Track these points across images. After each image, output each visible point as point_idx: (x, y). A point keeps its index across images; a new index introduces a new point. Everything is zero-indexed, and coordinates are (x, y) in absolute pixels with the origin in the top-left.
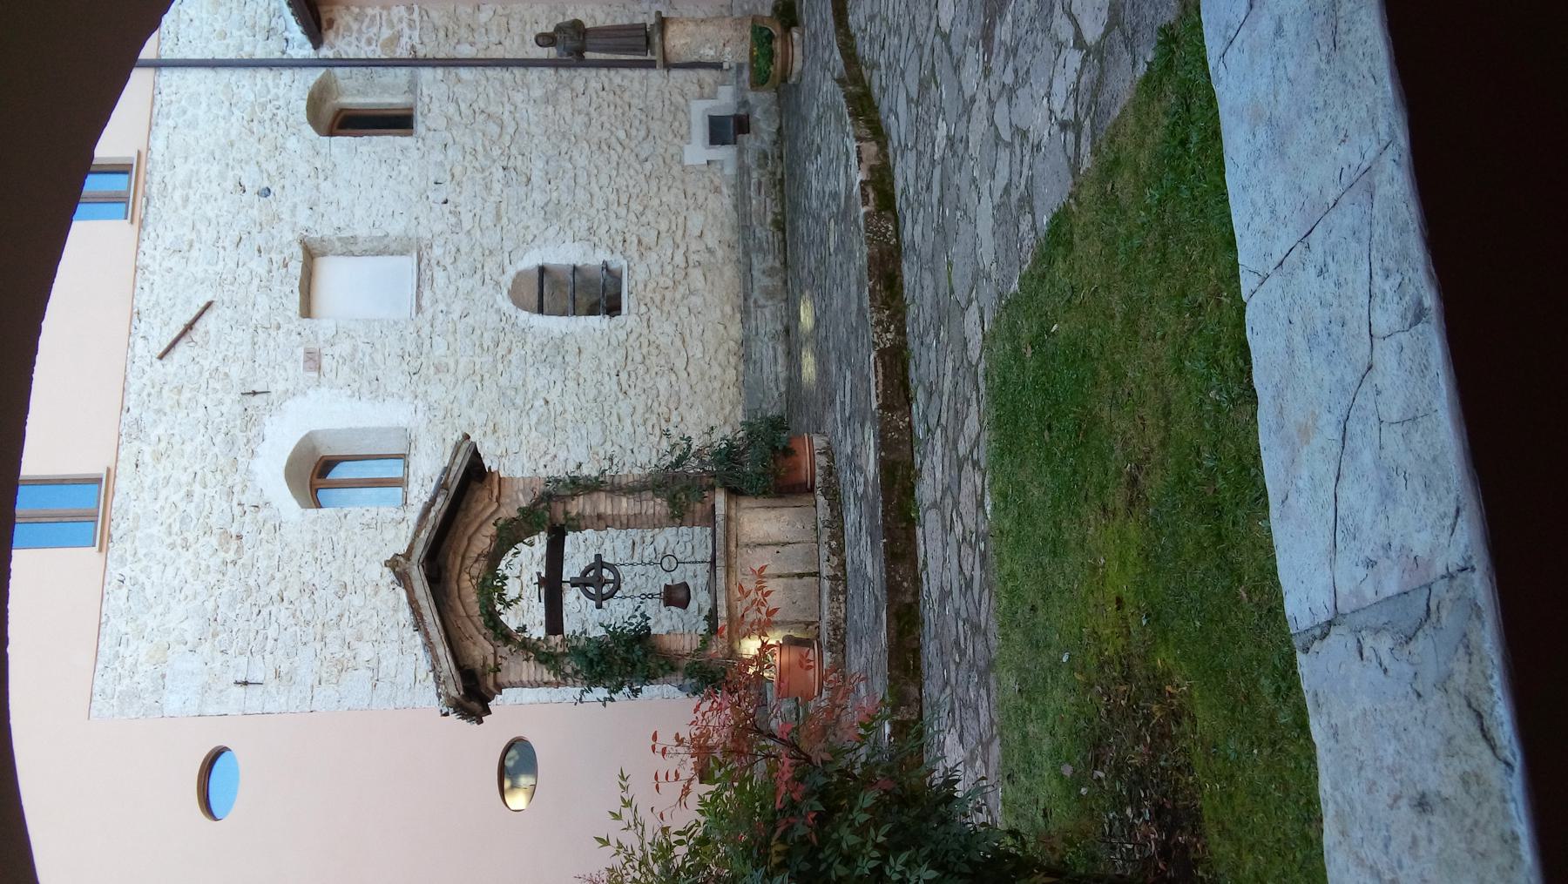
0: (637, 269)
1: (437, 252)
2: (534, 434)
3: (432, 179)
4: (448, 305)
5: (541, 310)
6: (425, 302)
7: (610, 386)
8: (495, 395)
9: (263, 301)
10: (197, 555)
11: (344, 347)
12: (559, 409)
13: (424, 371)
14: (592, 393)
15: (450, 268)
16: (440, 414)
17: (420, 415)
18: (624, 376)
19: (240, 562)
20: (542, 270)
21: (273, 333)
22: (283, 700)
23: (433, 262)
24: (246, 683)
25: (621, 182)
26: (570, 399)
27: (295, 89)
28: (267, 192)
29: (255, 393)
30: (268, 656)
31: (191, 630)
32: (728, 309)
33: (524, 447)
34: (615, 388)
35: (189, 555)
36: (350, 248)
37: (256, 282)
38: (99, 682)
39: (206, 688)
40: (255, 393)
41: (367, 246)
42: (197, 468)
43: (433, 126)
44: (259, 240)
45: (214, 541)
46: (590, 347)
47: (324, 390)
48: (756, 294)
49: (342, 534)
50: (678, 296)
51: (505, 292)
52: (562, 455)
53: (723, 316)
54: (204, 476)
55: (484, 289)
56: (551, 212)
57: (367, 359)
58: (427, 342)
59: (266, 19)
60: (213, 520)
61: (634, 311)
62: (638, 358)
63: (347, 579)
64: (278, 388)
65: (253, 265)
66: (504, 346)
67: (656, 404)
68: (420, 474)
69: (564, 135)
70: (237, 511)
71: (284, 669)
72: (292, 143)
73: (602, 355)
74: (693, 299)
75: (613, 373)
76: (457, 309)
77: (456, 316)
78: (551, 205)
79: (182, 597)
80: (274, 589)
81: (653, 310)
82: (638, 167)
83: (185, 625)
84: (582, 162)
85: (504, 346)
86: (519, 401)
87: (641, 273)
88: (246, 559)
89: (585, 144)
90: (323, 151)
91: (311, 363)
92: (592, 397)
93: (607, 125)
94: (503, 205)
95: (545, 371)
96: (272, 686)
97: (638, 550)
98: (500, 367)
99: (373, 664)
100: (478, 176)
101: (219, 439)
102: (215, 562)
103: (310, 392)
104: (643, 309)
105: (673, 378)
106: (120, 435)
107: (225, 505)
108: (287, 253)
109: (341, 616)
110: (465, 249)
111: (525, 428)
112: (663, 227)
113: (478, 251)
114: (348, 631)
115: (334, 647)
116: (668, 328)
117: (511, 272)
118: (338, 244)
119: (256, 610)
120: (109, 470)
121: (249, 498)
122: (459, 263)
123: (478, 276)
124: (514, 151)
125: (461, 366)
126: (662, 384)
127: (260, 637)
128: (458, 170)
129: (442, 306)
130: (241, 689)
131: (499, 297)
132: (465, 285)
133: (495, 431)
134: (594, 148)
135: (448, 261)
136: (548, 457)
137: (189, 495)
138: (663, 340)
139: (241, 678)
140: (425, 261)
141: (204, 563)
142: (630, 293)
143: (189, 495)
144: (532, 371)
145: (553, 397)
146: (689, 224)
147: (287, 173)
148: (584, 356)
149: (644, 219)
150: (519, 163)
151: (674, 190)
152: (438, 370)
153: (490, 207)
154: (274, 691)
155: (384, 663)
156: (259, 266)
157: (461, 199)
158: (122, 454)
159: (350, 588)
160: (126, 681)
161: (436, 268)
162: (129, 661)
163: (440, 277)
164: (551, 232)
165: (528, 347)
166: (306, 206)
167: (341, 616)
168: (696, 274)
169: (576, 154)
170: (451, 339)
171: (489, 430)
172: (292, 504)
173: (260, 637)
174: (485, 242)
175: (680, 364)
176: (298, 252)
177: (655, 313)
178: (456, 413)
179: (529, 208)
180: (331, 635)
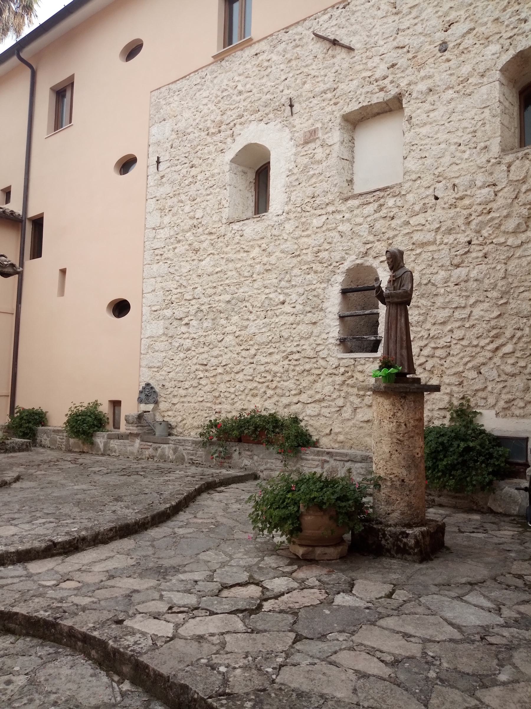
1: (391, 202)
2: (264, 297)
3: (457, 181)
4: (349, 220)
6: (350, 203)
7: (290, 347)
8: (287, 267)
12: (278, 312)
13: (304, 214)
14: (285, 334)
15: (377, 215)
16: (275, 232)
17: (275, 219)
18: (296, 356)
21: (332, 102)
22: (152, 184)
23: (382, 201)
25: (455, 349)
26: (283, 319)
30: (169, 170)
31: (181, 125)
32: (341, 438)
33: (256, 291)
34: (289, 350)
37: (369, 74)
38: (164, 88)
42: (255, 91)
43: (513, 168)
44: (402, 62)
45: (219, 118)
46: (316, 330)
47: (294, 150)
48: (332, 462)
49: (218, 190)
51: (359, 261)
52: (252, 317)
53: (337, 434)
55: (360, 244)
57: (311, 173)
58: (323, 212)
62: (307, 367)
63: (198, 200)
66: (319, 268)
67: (278, 379)
68: (245, 228)
69: (507, 293)
71: (164, 180)
72: (494, 48)
73: (311, 340)
75: (299, 349)
76: (344, 227)
77: (340, 228)
78: (434, 288)
81: (342, 378)
82: (470, 365)
84: (477, 312)
85: (319, 268)
86: (283, 283)
88: (209, 139)
90: (485, 79)
93: (519, 334)
95: (301, 300)
96: (158, 177)
97: (202, 368)
98: (305, 267)
100: (460, 221)
101: (269, 96)
102: (209, 124)
103: (292, 143)
104: (342, 370)
105: (293, 392)
106: (271, 35)
107: (234, 117)
110: (394, 223)
111: (267, 291)
113: (391, 234)
115: (170, 202)
116: (328, 389)
119: (187, 155)
120: (251, 39)
122: (382, 222)
123: (371, 238)
124: (487, 249)
125: (306, 240)
126: (290, 384)
127: (176, 162)
128: (466, 202)
129: (347, 216)
132: (363, 230)
133: (267, 271)
136: (251, 308)
138: (318, 385)
140: (381, 194)
143: (240, 93)
144: (301, 290)
145: (287, 308)
148: (310, 326)
150: (474, 255)
152: (303, 223)
153: (430, 237)
154: (156, 178)
155: (162, 231)
156: (382, 70)
157: (439, 211)
158: (263, 43)
159: (193, 203)
160: (164, 102)
161: (376, 205)
162: (171, 100)
165: (318, 285)
166: (431, 86)
169: (486, 305)
170: (324, 228)
171: (268, 267)
173: (176, 162)
174: (399, 238)
175: (303, 398)
176: (393, 91)
177: (339, 379)
178: (278, 242)
179: (431, 270)
180: (175, 200)
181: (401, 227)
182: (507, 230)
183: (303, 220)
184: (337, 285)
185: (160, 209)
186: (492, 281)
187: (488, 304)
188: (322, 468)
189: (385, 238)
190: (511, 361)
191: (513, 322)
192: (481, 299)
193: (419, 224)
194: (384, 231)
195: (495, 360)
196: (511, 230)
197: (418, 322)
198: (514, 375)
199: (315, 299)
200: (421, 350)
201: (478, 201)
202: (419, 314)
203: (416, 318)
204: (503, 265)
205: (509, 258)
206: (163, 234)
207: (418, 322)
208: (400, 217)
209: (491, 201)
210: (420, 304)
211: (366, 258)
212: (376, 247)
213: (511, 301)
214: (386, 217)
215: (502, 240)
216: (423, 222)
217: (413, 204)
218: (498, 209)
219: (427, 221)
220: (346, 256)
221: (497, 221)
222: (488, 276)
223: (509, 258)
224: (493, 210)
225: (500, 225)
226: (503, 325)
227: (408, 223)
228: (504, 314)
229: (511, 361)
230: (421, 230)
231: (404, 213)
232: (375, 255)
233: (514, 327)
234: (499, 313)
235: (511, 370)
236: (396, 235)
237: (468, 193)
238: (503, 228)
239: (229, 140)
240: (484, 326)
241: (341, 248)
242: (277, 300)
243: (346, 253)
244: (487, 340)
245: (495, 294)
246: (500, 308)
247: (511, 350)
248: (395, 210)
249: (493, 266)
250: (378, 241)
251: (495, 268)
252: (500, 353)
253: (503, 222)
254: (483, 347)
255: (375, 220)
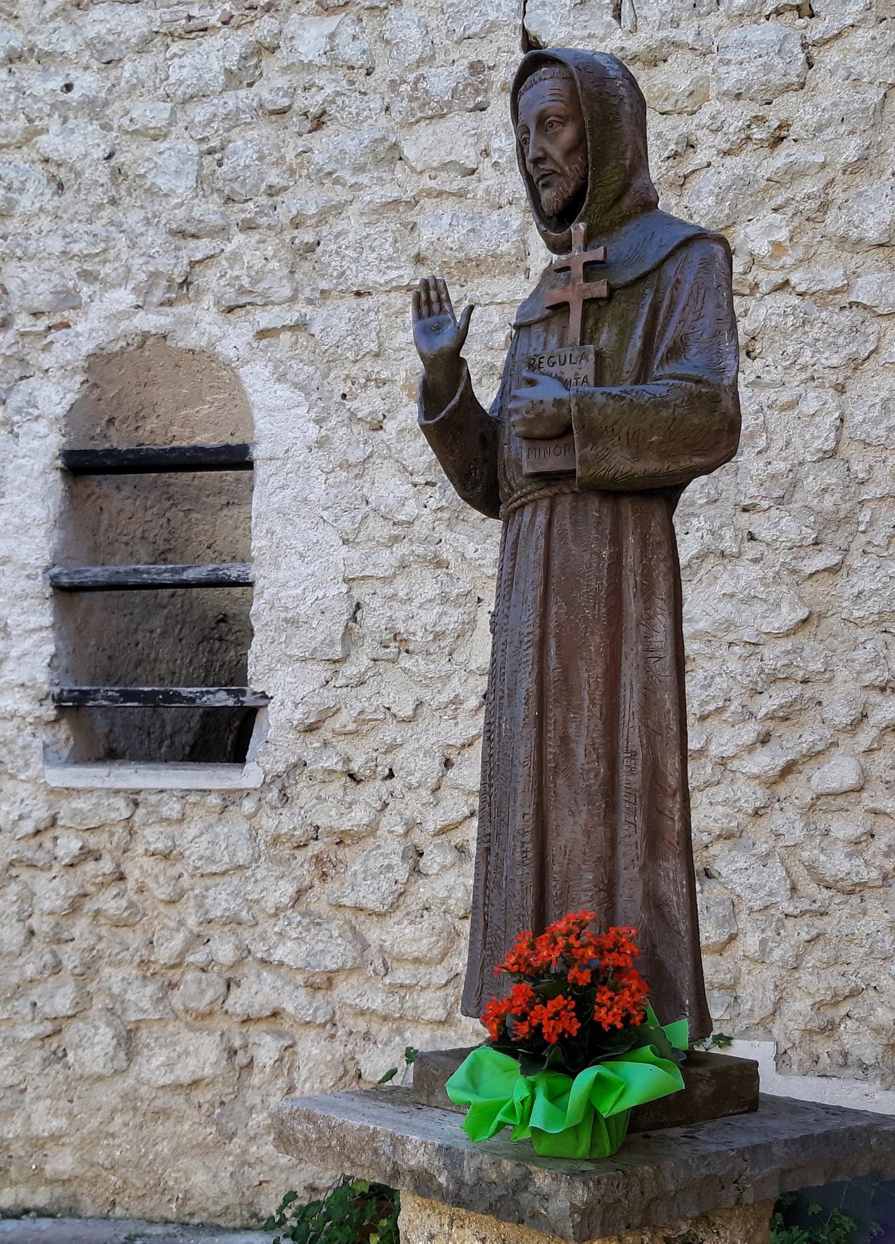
0: (234, 828)
4: (93, 108)
5: (81, 466)
15: (243, 96)
20: (237, 459)
51: (151, 321)
55: (154, 238)
61: (65, 809)
76: (77, 143)
77: (51, 142)
87: (230, 839)
89: (789, 615)
110: (323, 146)
113: (305, 199)
117: (233, 340)
122: (263, 132)
123: (209, 210)
131: (124, 297)
132: (171, 168)
134: (773, 655)
135: (272, 86)
142: (134, 799)
168: (202, 1054)
169: (747, 574)
174: (352, 224)
181: (360, 169)
182: (854, 234)
184: (41, 427)
186: (780, 466)
187: (756, 571)
189: (283, 215)
190: (844, 828)
191: (861, 656)
192: (728, 544)
193: (444, 166)
194: (274, 177)
195: (777, 820)
196: (873, 235)
197: (438, 636)
198: (856, 889)
200: (448, 764)
201: (733, 77)
202: (444, 599)
203: (429, 617)
204: (829, 395)
205: (856, 364)
207: (438, 636)
208: (357, 120)
209: (788, 88)
210: (447, 554)
211: (183, 309)
212: (235, 258)
213: (855, 561)
214: (282, 112)
215: (833, 278)
216: (468, 156)
217: (420, 62)
218: (820, 128)
219: (486, 153)
220: (86, 290)
221: (811, 186)
222: (762, 443)
223: (856, 364)
224: (796, 130)
225: (824, 207)
226: (817, 666)
227: (394, 155)
228: (821, 616)
229: (844, 828)
230: (461, 195)
231: (376, 104)
232: (230, 296)
233: (868, 678)
234: (802, 613)
235: (847, 866)
236: (338, 209)
237: (687, 34)
238: (835, 222)
240: (734, 666)
241: (56, 244)
243: (87, 276)
244: (749, 733)
245: (788, 527)
246: (808, 588)
247: (851, 779)
248: (329, 84)
249: (785, 397)
250: (248, 227)
251: (792, 405)
252: (800, 789)
253: (837, 194)
254: (723, 762)
255: (233, 120)
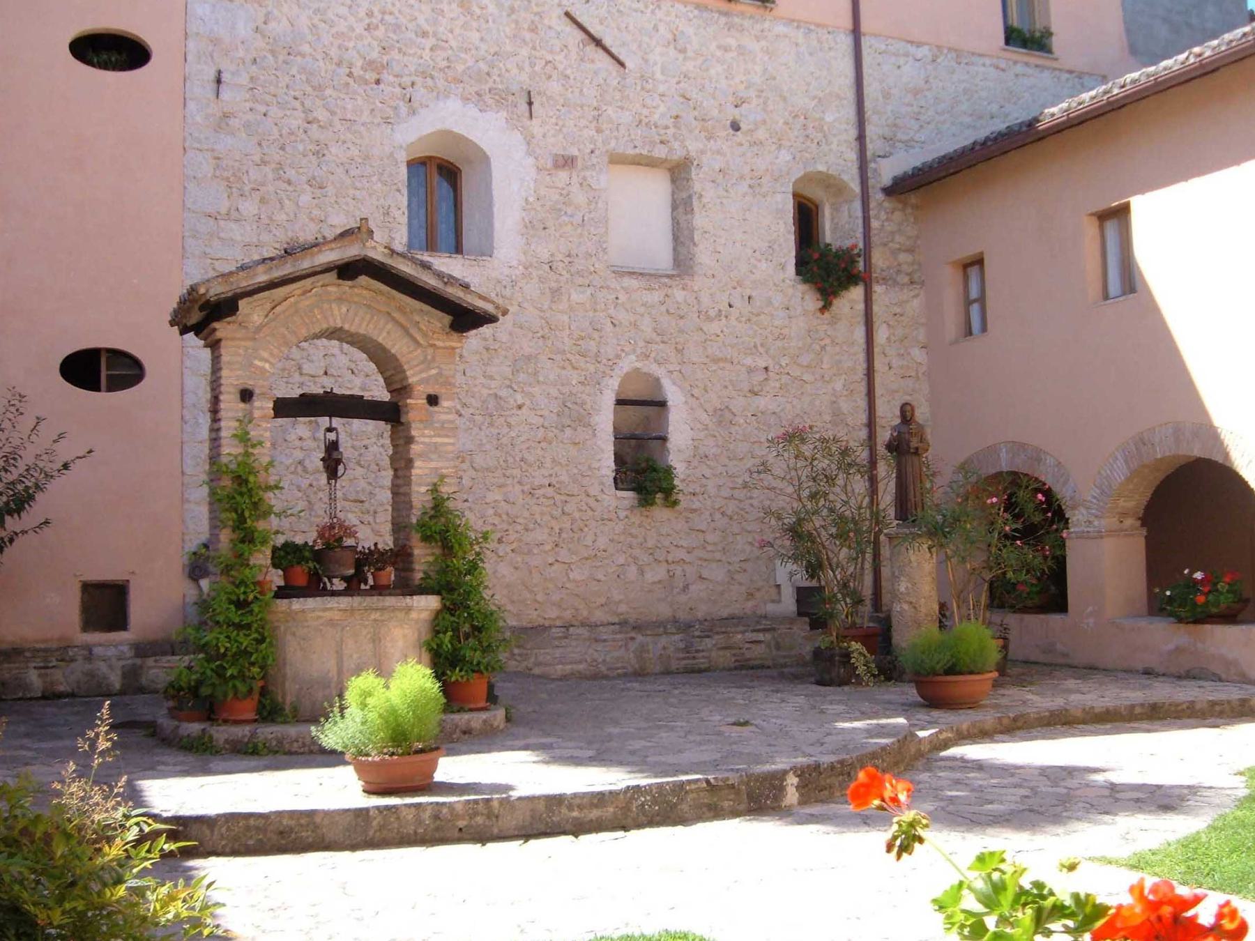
1: (679, 295)
5: (620, 402)
9: (626, 117)
10: (360, 37)
11: (580, 198)
12: (512, 421)
19: (351, 81)
20: (662, 404)
24: (219, 81)
27: (838, 158)
28: (736, 127)
29: (530, 104)
32: (623, 608)
35: (359, 29)
36: (681, 206)
39: (216, 41)
40: (530, 104)
41: (683, 225)
45: (374, 55)
48: (640, 638)
50: (637, 552)
51: (638, 365)
54: (443, 49)
56: (723, 416)
59: (905, 138)
60: (395, 55)
64: (535, 126)
65: (662, 109)
70: (406, 80)
74: (633, 569)
76: (623, 316)
79: (316, 21)
80: (321, 114)
83: (285, 22)
91: (561, 162)
92: (526, 456)
94: (728, 366)
99: (234, 214)
103: (531, 161)
108: (676, 145)
109: (289, 182)
112: (711, 538)
114: (271, 189)
115: (254, 174)
118: (684, 195)
121: (420, 93)
126: (540, 535)
127: (268, 98)
129: (623, 298)
130: (212, 75)
132: (646, 325)
137: (425, 34)
139: (226, 77)
141: (351, 45)
143: (425, 34)
146: (714, 565)
147: (755, 149)
149: (718, 516)
151: (748, 548)
155: (233, 225)
157: (733, 322)
163: (656, 296)
164: (704, 417)
165: (581, 388)
167: (289, 182)
172: (412, 137)
183: (554, 285)
185: (227, 179)
188: (627, 650)
199: (576, 407)
206: (235, 231)
216: (719, 332)
239: (404, 109)
242: (512, 402)
